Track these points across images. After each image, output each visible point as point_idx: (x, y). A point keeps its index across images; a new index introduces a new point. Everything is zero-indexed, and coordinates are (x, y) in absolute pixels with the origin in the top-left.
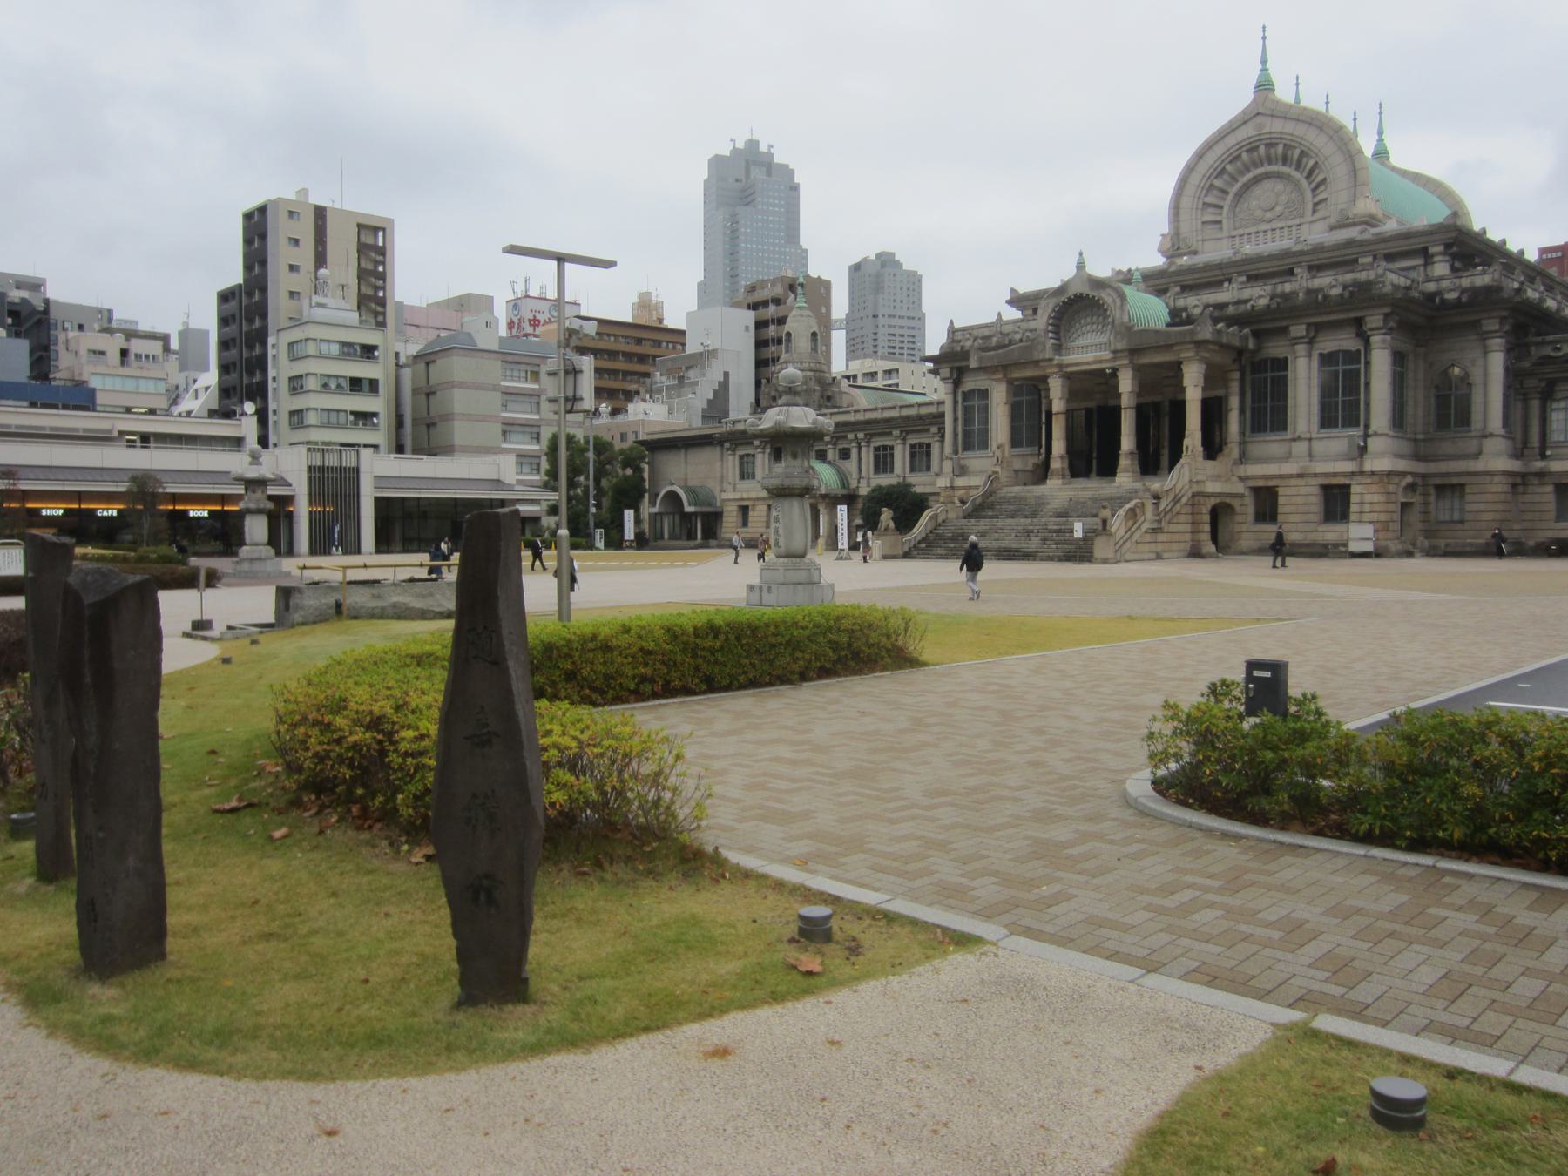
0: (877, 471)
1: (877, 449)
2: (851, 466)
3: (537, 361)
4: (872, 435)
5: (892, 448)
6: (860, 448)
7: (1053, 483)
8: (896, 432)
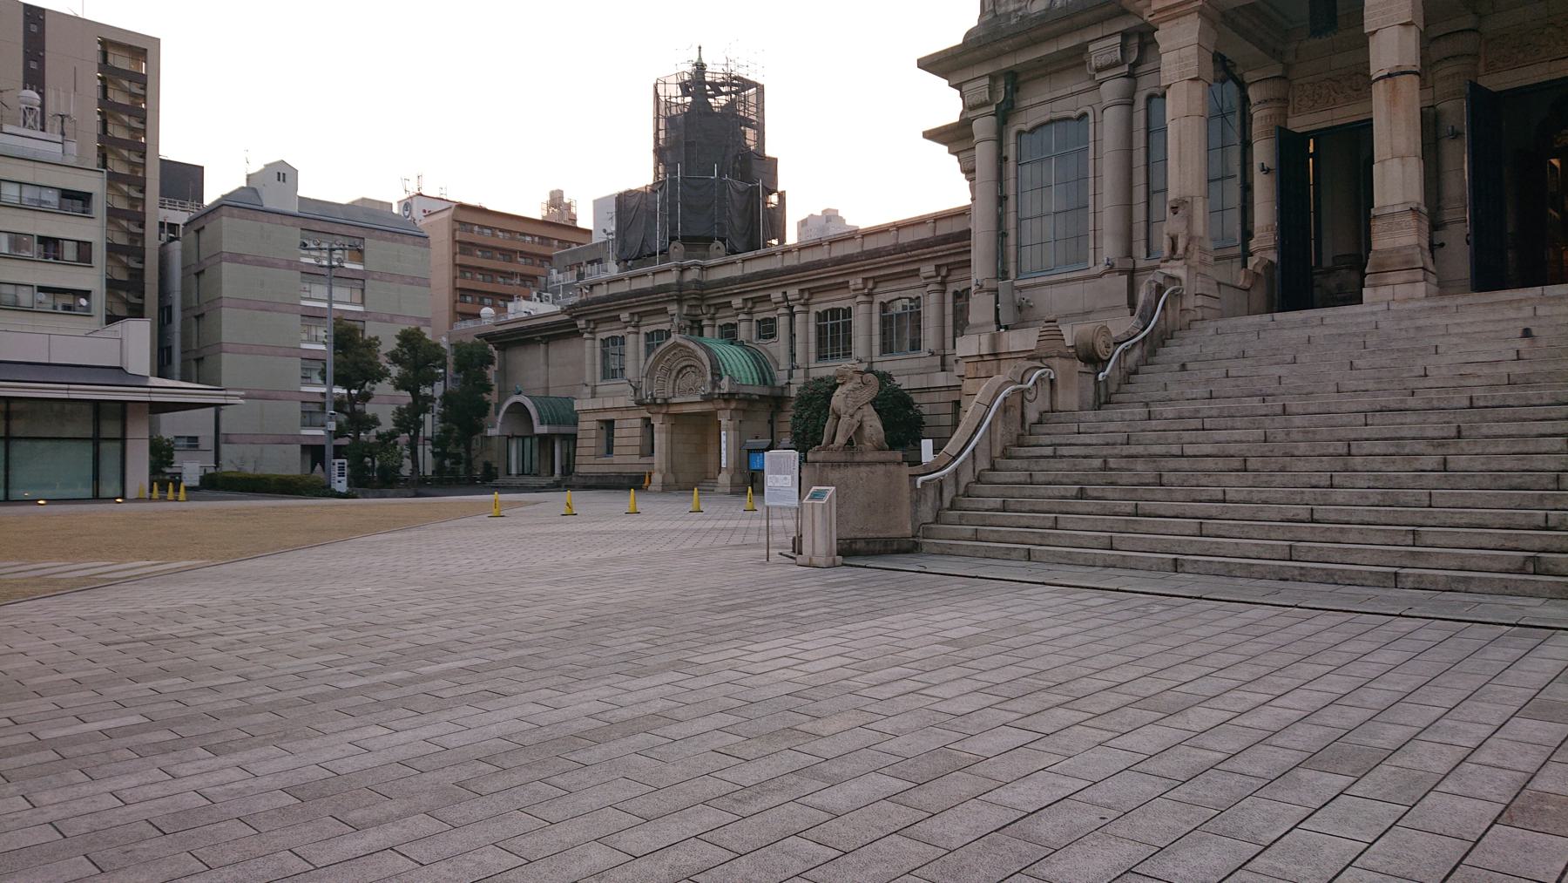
0: (821, 357)
1: (821, 316)
2: (777, 348)
3: (359, 233)
4: (812, 292)
5: (848, 312)
6: (792, 315)
7: (1393, 301)
8: (856, 282)
